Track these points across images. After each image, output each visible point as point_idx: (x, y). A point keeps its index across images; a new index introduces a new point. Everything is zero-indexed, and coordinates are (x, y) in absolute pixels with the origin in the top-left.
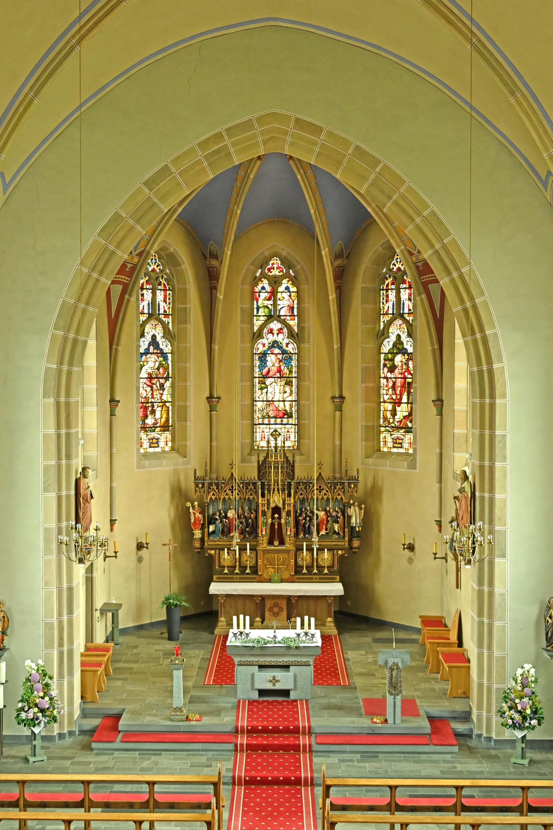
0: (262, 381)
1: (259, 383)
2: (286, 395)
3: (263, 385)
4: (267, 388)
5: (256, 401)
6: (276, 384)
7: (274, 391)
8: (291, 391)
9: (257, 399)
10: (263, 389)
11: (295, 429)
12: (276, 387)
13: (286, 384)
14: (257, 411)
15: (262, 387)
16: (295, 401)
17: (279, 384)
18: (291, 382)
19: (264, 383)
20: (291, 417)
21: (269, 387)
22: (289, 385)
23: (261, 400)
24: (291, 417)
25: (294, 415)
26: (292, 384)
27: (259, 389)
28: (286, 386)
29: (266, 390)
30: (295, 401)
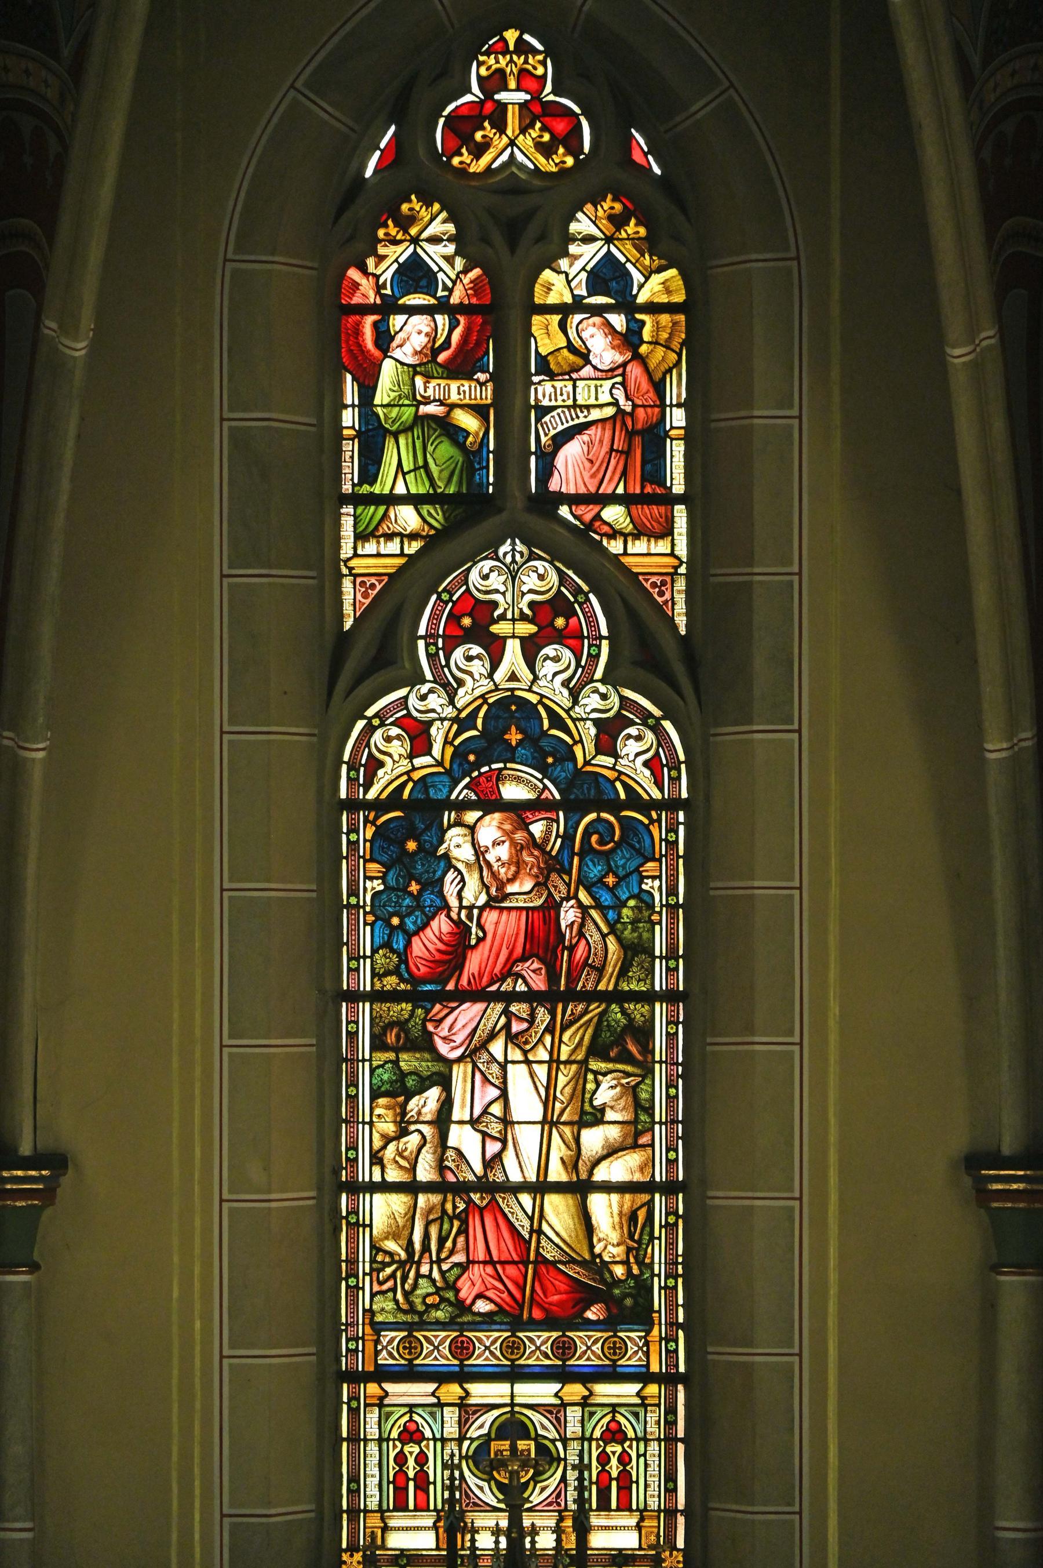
0: (401, 1025)
1: (378, 1044)
2: (593, 1140)
3: (408, 1062)
4: (445, 1082)
5: (355, 1188)
6: (515, 1054)
7: (496, 1109)
8: (642, 1107)
9: (367, 1172)
10: (409, 1096)
11: (672, 1410)
12: (517, 1075)
13: (597, 1050)
14: (364, 1266)
15: (403, 1075)
16: (669, 1188)
17: (542, 1054)
18: (644, 1034)
19: (425, 1044)
20: (643, 1317)
21: (460, 1074)
22: (625, 1057)
23: (393, 1175)
24: (643, 1317)
25: (658, 1300)
26: (647, 1049)
27: (375, 1095)
28: (595, 1065)
29: (434, 1094)
30: (669, 1188)
